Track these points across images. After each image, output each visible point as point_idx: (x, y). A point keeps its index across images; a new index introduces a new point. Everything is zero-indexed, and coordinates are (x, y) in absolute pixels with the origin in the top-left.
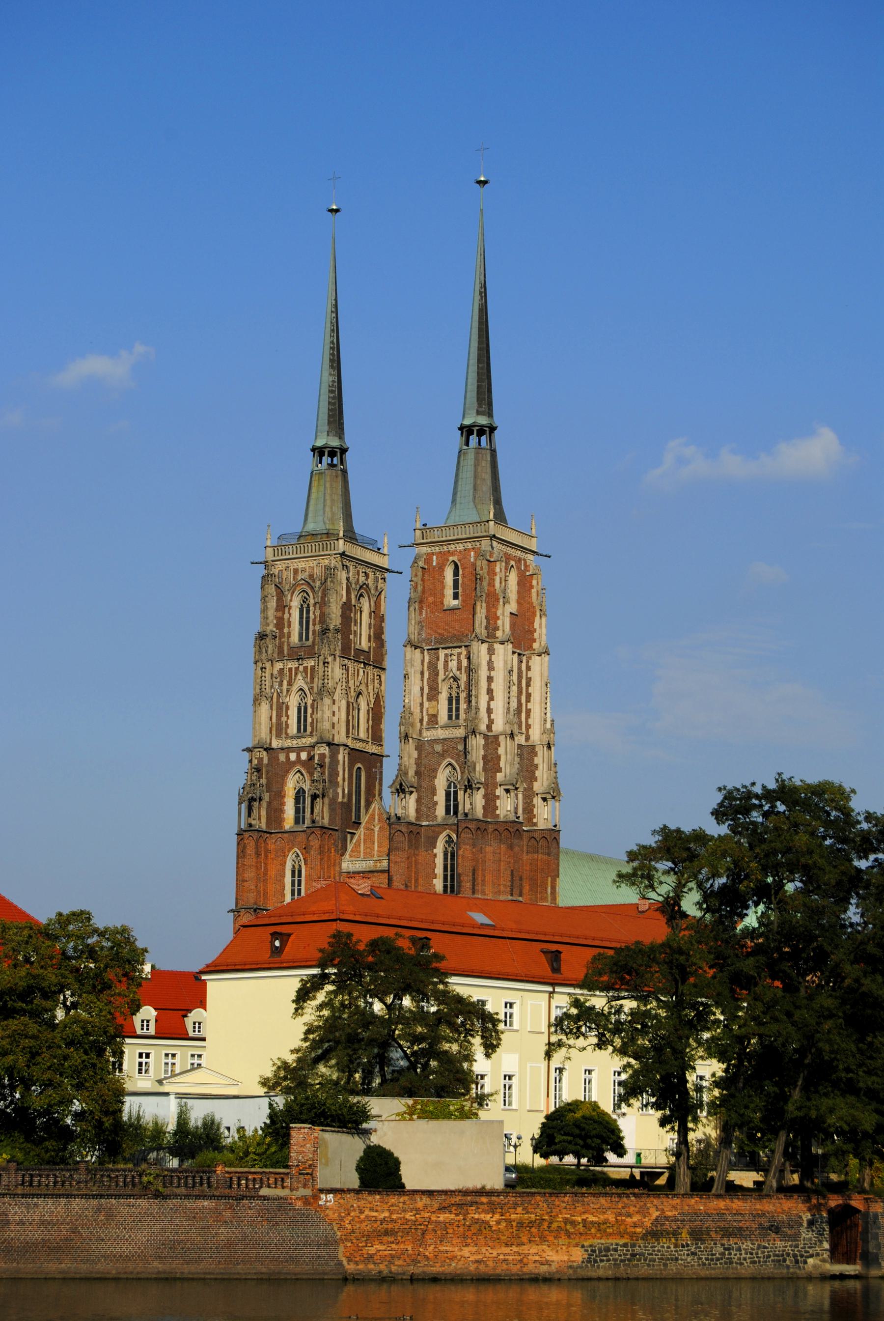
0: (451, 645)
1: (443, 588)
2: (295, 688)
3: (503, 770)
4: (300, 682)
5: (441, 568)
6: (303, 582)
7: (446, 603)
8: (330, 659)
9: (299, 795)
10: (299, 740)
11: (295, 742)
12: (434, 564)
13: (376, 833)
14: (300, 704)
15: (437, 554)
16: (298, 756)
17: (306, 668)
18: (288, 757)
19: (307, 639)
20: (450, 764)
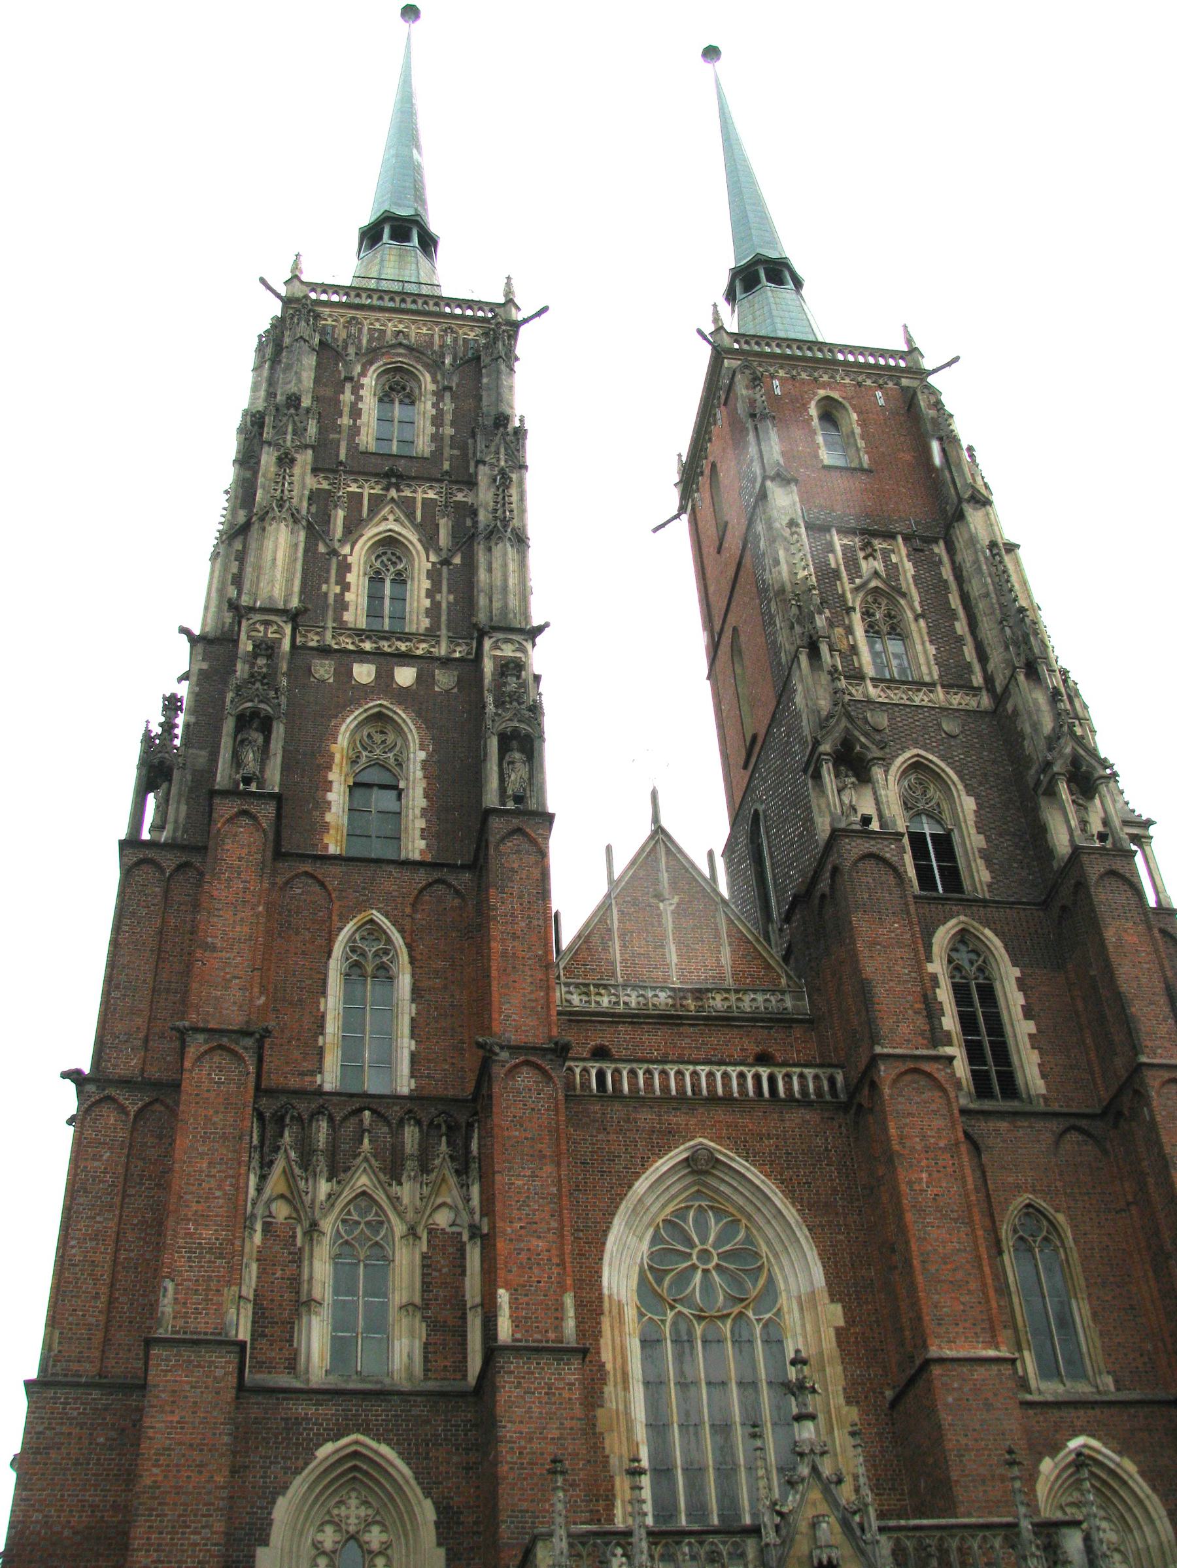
2: (372, 532)
6: (401, 351)
11: (368, 646)
13: (669, 921)
14: (378, 572)
16: (384, 679)
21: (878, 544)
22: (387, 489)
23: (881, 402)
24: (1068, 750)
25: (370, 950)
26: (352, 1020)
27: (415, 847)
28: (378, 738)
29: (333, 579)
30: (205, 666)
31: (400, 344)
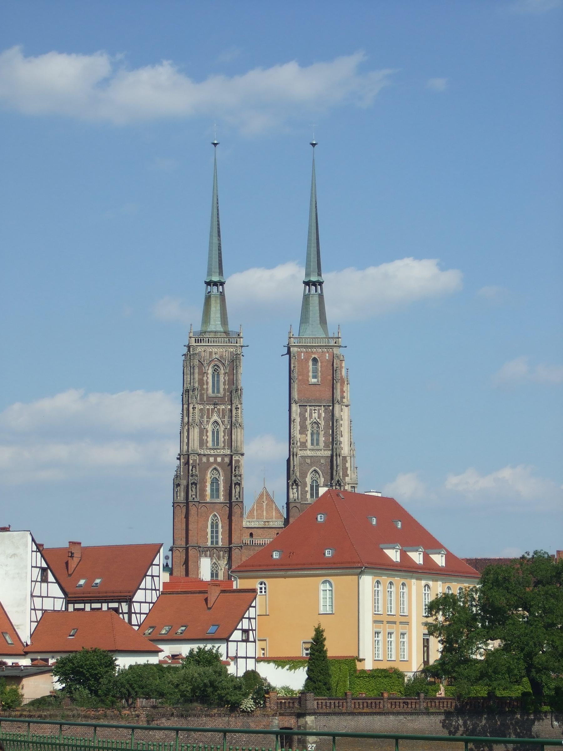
0: (314, 404)
1: (309, 372)
2: (212, 421)
3: (349, 475)
4: (215, 417)
5: (307, 360)
6: (216, 359)
7: (310, 380)
8: (239, 406)
9: (215, 481)
10: (215, 450)
11: (212, 451)
12: (302, 358)
13: (265, 506)
14: (213, 429)
15: (304, 352)
16: (215, 460)
17: (219, 410)
18: (208, 460)
19: (218, 392)
20: (315, 470)
21: (317, 408)
22: (215, 407)
23: (327, 358)
24: (337, 479)
25: (215, 519)
26: (212, 532)
27: (222, 499)
28: (215, 471)
29: (205, 436)
30: (183, 461)
31: (216, 358)
